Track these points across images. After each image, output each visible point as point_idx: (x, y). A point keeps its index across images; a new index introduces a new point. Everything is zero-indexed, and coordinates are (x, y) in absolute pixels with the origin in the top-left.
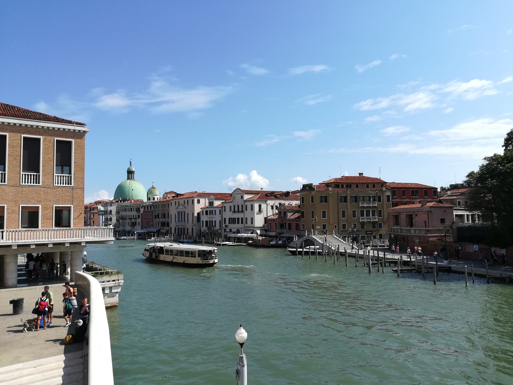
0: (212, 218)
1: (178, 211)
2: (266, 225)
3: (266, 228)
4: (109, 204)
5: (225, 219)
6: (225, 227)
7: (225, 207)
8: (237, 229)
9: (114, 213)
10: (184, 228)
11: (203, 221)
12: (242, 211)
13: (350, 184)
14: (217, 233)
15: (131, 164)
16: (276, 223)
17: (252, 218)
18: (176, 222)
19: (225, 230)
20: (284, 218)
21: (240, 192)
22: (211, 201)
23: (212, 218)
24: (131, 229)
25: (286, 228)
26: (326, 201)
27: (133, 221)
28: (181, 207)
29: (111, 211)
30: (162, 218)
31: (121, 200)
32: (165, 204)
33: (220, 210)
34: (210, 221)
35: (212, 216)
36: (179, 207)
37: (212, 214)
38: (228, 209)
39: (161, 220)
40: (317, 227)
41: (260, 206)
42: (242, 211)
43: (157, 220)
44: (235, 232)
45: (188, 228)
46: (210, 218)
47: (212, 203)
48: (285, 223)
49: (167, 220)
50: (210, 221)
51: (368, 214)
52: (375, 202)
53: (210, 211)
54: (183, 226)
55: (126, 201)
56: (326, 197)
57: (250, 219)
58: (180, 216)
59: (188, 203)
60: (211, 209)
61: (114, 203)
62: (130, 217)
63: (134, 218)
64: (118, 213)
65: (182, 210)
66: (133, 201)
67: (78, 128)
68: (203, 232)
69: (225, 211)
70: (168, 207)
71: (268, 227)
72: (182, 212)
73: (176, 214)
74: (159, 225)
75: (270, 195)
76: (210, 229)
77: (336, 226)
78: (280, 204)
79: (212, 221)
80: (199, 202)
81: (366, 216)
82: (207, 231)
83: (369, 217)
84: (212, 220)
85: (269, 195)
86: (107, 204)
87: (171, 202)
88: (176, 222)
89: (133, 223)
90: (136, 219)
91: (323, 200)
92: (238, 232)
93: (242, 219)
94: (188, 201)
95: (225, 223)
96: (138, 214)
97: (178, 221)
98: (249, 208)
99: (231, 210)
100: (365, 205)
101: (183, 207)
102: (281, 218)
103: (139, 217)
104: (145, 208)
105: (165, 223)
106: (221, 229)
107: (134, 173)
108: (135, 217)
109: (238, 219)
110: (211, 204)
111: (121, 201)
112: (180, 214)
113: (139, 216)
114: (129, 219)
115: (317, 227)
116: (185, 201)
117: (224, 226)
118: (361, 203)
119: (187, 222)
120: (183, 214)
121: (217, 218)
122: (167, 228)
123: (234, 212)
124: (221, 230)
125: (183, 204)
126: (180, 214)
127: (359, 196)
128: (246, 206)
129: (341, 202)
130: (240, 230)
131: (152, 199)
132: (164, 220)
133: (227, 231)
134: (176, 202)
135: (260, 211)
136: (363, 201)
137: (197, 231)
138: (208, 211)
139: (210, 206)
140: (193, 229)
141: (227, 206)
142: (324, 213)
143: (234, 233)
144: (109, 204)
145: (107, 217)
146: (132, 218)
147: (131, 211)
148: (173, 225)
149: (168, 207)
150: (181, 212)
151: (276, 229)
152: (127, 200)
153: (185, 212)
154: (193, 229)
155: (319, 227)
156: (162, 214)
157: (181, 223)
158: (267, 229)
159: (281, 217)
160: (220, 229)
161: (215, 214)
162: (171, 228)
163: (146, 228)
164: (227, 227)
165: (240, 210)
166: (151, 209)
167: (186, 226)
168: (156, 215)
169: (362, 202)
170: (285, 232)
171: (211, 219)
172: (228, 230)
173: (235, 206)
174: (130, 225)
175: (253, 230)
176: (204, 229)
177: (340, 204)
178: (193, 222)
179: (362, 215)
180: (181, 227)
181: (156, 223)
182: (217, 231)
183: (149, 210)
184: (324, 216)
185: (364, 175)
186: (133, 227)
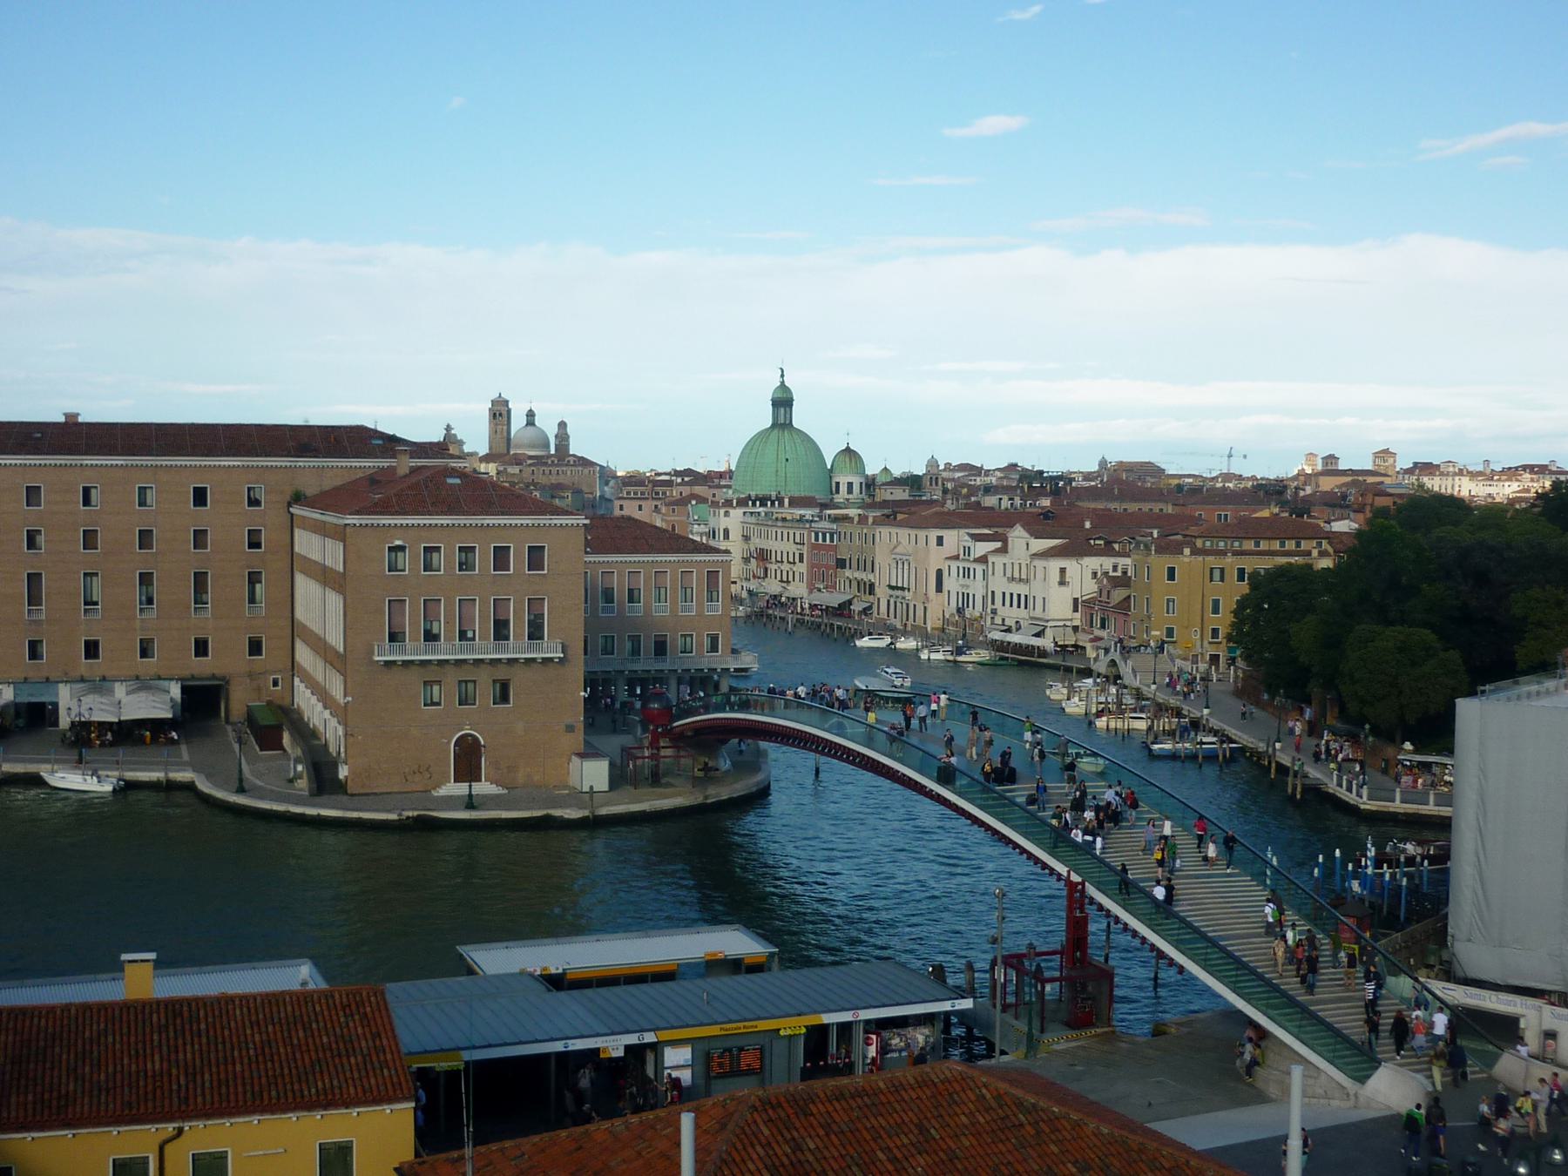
0: (968, 586)
3: (1077, 623)
4: (722, 511)
5: (993, 592)
9: (735, 535)
10: (907, 605)
12: (1027, 581)
15: (782, 376)
17: (1044, 599)
22: (967, 544)
29: (726, 532)
38: (999, 569)
41: (1063, 571)
42: (1027, 581)
46: (963, 586)
49: (871, 577)
58: (900, 571)
60: (967, 565)
61: (735, 508)
63: (788, 562)
64: (746, 538)
65: (905, 558)
66: (786, 501)
78: (1115, 568)
80: (940, 541)
95: (993, 603)
98: (1040, 575)
103: (801, 560)
110: (967, 551)
111: (754, 504)
112: (900, 566)
113: (801, 556)
120: (906, 567)
121: (977, 588)
126: (900, 566)
135: (1062, 583)
143: (1009, 630)
144: (722, 511)
146: (785, 559)
155: (1158, 633)
163: (819, 590)
166: (832, 540)
174: (779, 578)
183: (828, 542)
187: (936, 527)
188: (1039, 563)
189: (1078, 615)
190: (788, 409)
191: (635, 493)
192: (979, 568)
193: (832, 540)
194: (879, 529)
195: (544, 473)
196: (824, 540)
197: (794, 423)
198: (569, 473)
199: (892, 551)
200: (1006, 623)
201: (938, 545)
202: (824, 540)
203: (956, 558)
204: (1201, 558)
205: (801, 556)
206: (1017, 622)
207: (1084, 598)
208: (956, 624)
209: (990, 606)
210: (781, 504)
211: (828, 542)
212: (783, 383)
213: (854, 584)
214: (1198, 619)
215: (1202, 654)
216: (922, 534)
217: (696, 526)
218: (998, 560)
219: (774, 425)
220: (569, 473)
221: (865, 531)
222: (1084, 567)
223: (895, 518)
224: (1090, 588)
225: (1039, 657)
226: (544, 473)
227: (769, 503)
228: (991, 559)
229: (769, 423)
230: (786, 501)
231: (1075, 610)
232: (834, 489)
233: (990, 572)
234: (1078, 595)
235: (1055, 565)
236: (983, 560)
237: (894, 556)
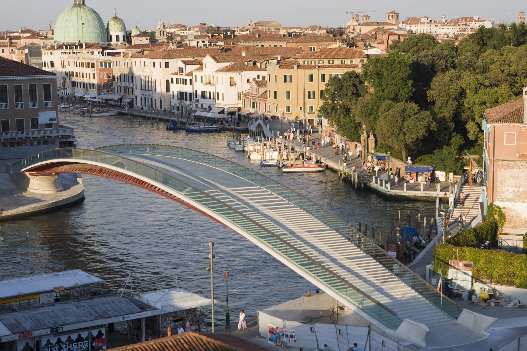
2: (241, 102)
10: (152, 99)
17: (223, 93)
19: (196, 105)
38: (199, 79)
39: (123, 84)
45: (155, 99)
49: (131, 85)
53: (180, 79)
57: (222, 94)
65: (149, 74)
67: (53, 77)
68: (173, 106)
80: (167, 65)
82: (178, 105)
93: (214, 93)
99: (202, 82)
110: (181, 70)
111: (66, 48)
113: (94, 75)
130: (212, 106)
140: (161, 101)
142: (288, 93)
154: (161, 101)
155: (282, 109)
162: (136, 97)
166: (110, 66)
172: (199, 106)
175: (223, 108)
180: (147, 97)
187: (165, 57)
193: (110, 66)
194: (134, 59)
196: (106, 66)
197: (85, 3)
200: (204, 107)
202: (106, 66)
203: (176, 74)
205: (94, 75)
206: (209, 106)
207: (244, 93)
209: (195, 99)
213: (123, 89)
218: (198, 74)
223: (143, 54)
224: (247, 87)
227: (74, 47)
228: (195, 73)
230: (84, 46)
232: (109, 39)
236: (190, 74)
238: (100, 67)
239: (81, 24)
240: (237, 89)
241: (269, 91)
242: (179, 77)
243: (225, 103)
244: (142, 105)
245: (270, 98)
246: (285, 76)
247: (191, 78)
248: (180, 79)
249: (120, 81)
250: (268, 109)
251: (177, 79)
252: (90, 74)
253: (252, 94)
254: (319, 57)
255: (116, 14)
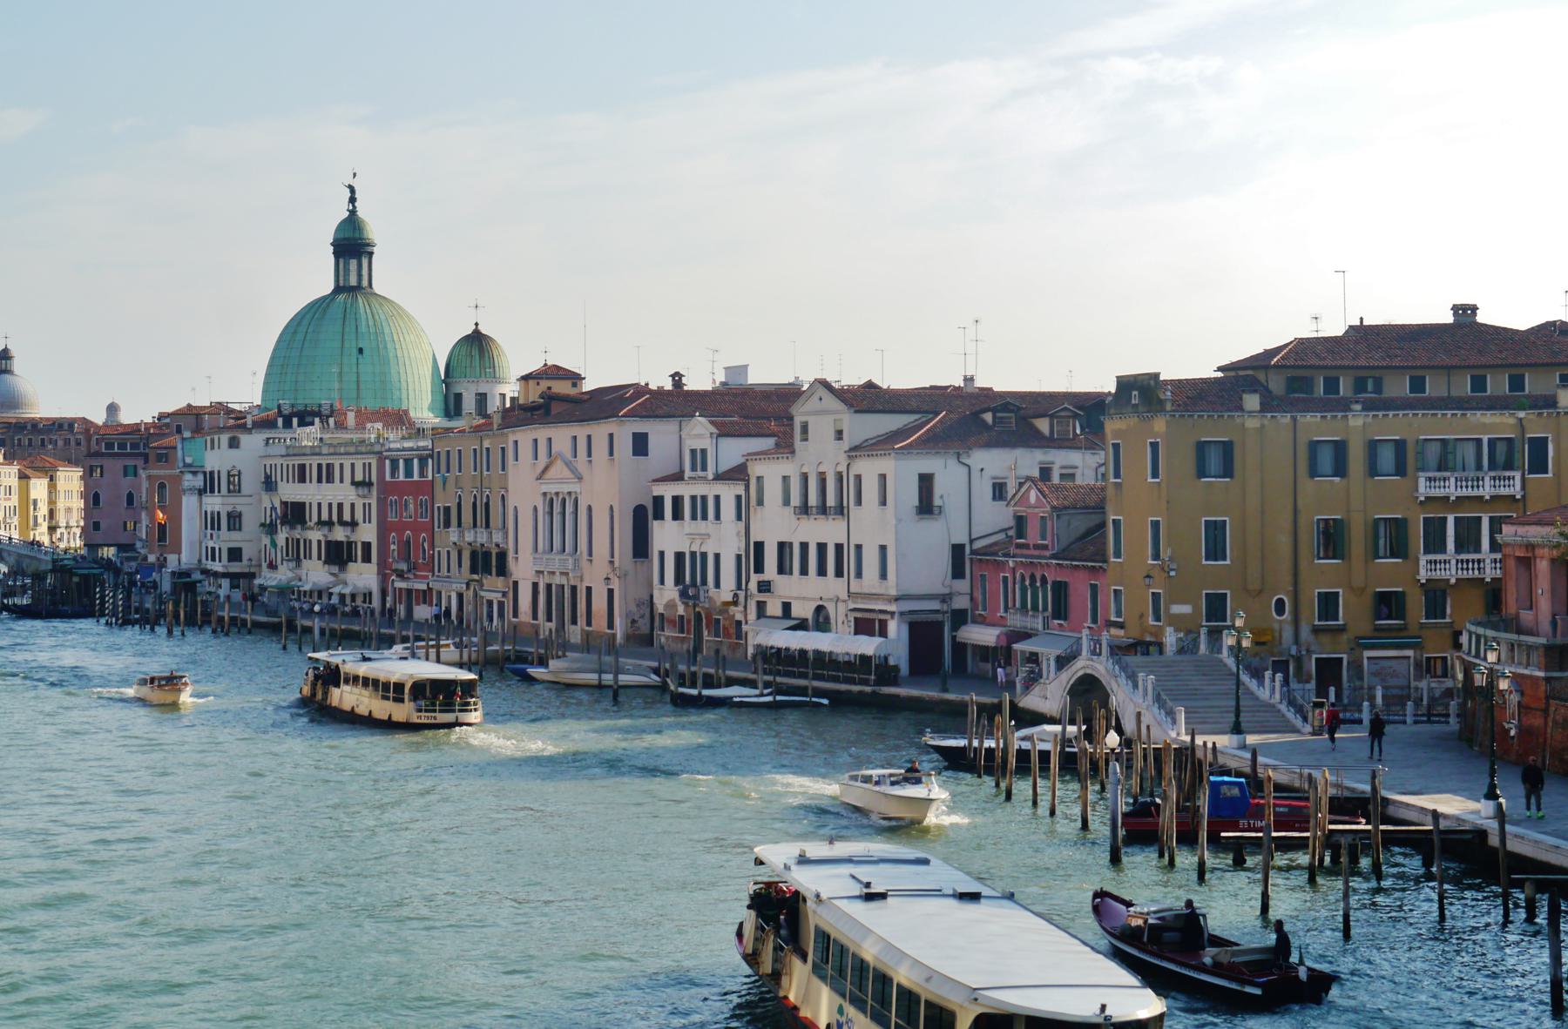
0: (705, 537)
1: (545, 494)
3: (961, 603)
4: (225, 438)
5: (759, 546)
6: (760, 591)
7: (759, 479)
8: (814, 605)
10: (574, 589)
11: (662, 554)
12: (841, 510)
13: (1377, 373)
14: (727, 623)
15: (352, 200)
16: (1005, 579)
18: (536, 549)
19: (761, 606)
20: (1037, 553)
21: (832, 403)
22: (698, 445)
23: (705, 537)
24: (332, 579)
25: (1045, 609)
26: (1228, 471)
27: (340, 534)
28: (559, 470)
30: (475, 525)
31: (286, 412)
32: (488, 449)
33: (738, 498)
34: (693, 554)
35: (700, 526)
36: (552, 473)
37: (705, 517)
38: (773, 491)
39: (469, 537)
40: (1177, 609)
41: (926, 481)
42: (841, 510)
43: (453, 535)
44: (807, 620)
45: (589, 589)
47: (704, 452)
48: (1044, 580)
49: (497, 537)
50: (693, 554)
51: (1468, 538)
52: (1507, 474)
53: (693, 498)
54: (566, 574)
55: (317, 420)
56: (1227, 448)
58: (557, 518)
59: (589, 455)
60: (699, 490)
61: (249, 431)
62: (325, 517)
63: (342, 523)
65: (565, 488)
66: (351, 419)
69: (760, 502)
70: (503, 469)
71: (972, 599)
72: (564, 501)
73: (535, 509)
74: (460, 565)
75: (994, 417)
76: (689, 598)
77: (1280, 603)
78: (1045, 472)
79: (704, 555)
80: (640, 445)
81: (1459, 548)
82: (681, 610)
83: (1476, 556)
84: (703, 550)
85: (988, 417)
86: (216, 437)
87: (516, 442)
88: (536, 549)
89: (339, 544)
90: (353, 524)
91: (1214, 460)
92: (821, 620)
93: (839, 547)
94: (589, 437)
95: (759, 568)
96: (364, 497)
97: (547, 547)
99: (787, 502)
100: (1452, 490)
101: (567, 473)
102: (1025, 552)
104: (394, 463)
105: (491, 553)
106: (742, 599)
107: (371, 254)
108: (347, 517)
109: (822, 548)
112: (557, 509)
114: (320, 523)
115: (1177, 609)
116: (575, 437)
117: (753, 586)
118: (1430, 479)
119: (585, 556)
121: (724, 540)
122: (499, 583)
123: (805, 509)
124: (741, 608)
125: (568, 455)
126: (557, 509)
127: (1417, 441)
128: (858, 478)
129: (1313, 472)
130: (830, 608)
131: (469, 404)
132: (481, 537)
133: (768, 614)
134: (536, 441)
135: (926, 506)
136: (1439, 470)
137: (634, 608)
138: (683, 497)
139: (693, 474)
140: (611, 592)
141: (771, 473)
142: (1215, 531)
143: (802, 625)
144: (225, 438)
145: (217, 509)
146: (335, 518)
147: (330, 480)
148: (523, 569)
149: (503, 469)
150: (561, 497)
151: (1006, 609)
152: (319, 414)
153: (576, 501)
154: (611, 592)
156: (475, 505)
157: (556, 562)
158: (966, 610)
159: (1026, 546)
160: (735, 603)
161: (718, 517)
162: (516, 584)
164: (769, 591)
165: (831, 501)
167: (582, 581)
168: (447, 510)
169: (1431, 474)
170: (1040, 627)
171: (698, 542)
172: (774, 608)
173: (805, 477)
176: (666, 595)
177: (1308, 486)
178: (612, 556)
179: (1435, 542)
180: (557, 580)
181: (448, 552)
182: (727, 611)
183: (416, 477)
184: (1215, 550)
185: (1482, 318)
186: (335, 569)
188: (869, 469)
189: (963, 585)
190: (365, 262)
191: (122, 446)
192: (728, 493)
193: (422, 473)
194: (514, 435)
195: (19, 445)
198: (60, 443)
199: (539, 478)
201: (635, 454)
202: (409, 473)
203: (678, 477)
204: (1285, 419)
206: (820, 609)
207: (978, 545)
208: (681, 623)
209: (754, 578)
210: (341, 426)
211: (416, 477)
212: (353, 212)
214: (1288, 578)
215: (1299, 660)
216: (600, 431)
217: (188, 477)
218: (771, 473)
219: (338, 289)
220: (60, 443)
221: (486, 444)
222: (975, 474)
223: (548, 413)
224: (993, 518)
225: (879, 682)
226: (19, 445)
228: (756, 469)
229: (328, 287)
230: (351, 419)
231: (958, 572)
232: (452, 406)
233: (753, 501)
234: (961, 538)
235: (902, 472)
236: (738, 473)
237: (544, 488)
238: (388, 478)
239: (355, 351)
240: (951, 528)
241: (1116, 523)
242: (685, 490)
243: (893, 592)
244: (535, 617)
245: (1117, 554)
246: (1201, 447)
247: (740, 490)
248: (693, 498)
249: (459, 525)
250: (1107, 610)
251: (677, 501)
252: (353, 505)
253: (1019, 546)
254: (1362, 362)
255: (477, 324)
